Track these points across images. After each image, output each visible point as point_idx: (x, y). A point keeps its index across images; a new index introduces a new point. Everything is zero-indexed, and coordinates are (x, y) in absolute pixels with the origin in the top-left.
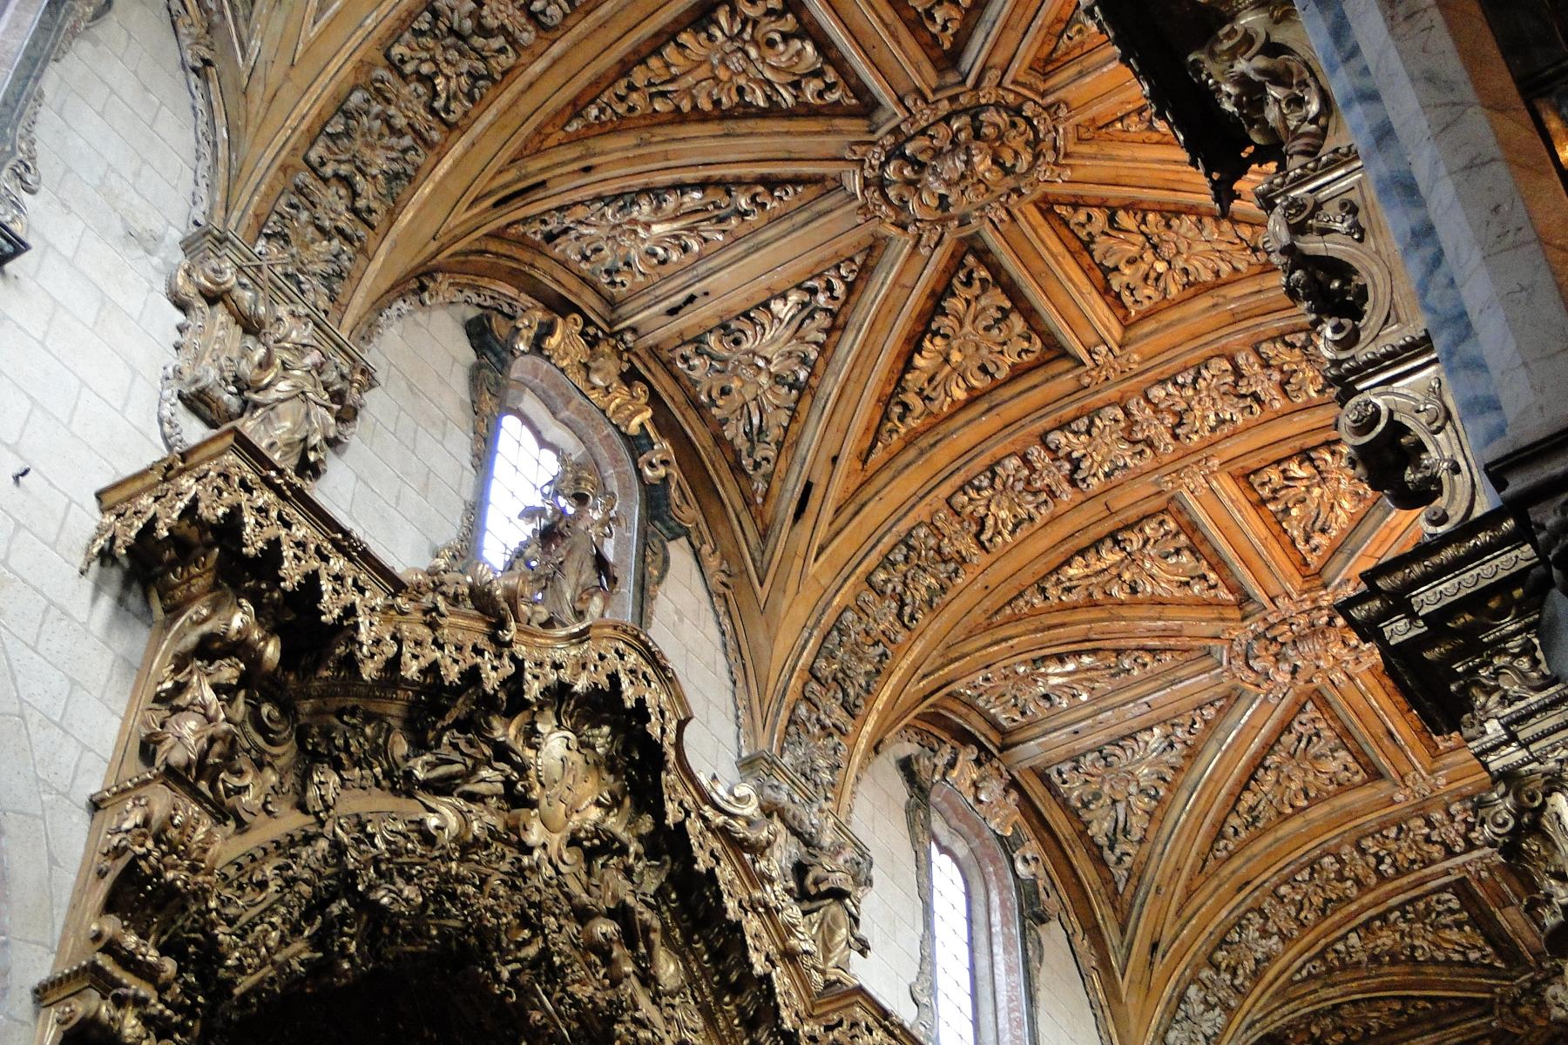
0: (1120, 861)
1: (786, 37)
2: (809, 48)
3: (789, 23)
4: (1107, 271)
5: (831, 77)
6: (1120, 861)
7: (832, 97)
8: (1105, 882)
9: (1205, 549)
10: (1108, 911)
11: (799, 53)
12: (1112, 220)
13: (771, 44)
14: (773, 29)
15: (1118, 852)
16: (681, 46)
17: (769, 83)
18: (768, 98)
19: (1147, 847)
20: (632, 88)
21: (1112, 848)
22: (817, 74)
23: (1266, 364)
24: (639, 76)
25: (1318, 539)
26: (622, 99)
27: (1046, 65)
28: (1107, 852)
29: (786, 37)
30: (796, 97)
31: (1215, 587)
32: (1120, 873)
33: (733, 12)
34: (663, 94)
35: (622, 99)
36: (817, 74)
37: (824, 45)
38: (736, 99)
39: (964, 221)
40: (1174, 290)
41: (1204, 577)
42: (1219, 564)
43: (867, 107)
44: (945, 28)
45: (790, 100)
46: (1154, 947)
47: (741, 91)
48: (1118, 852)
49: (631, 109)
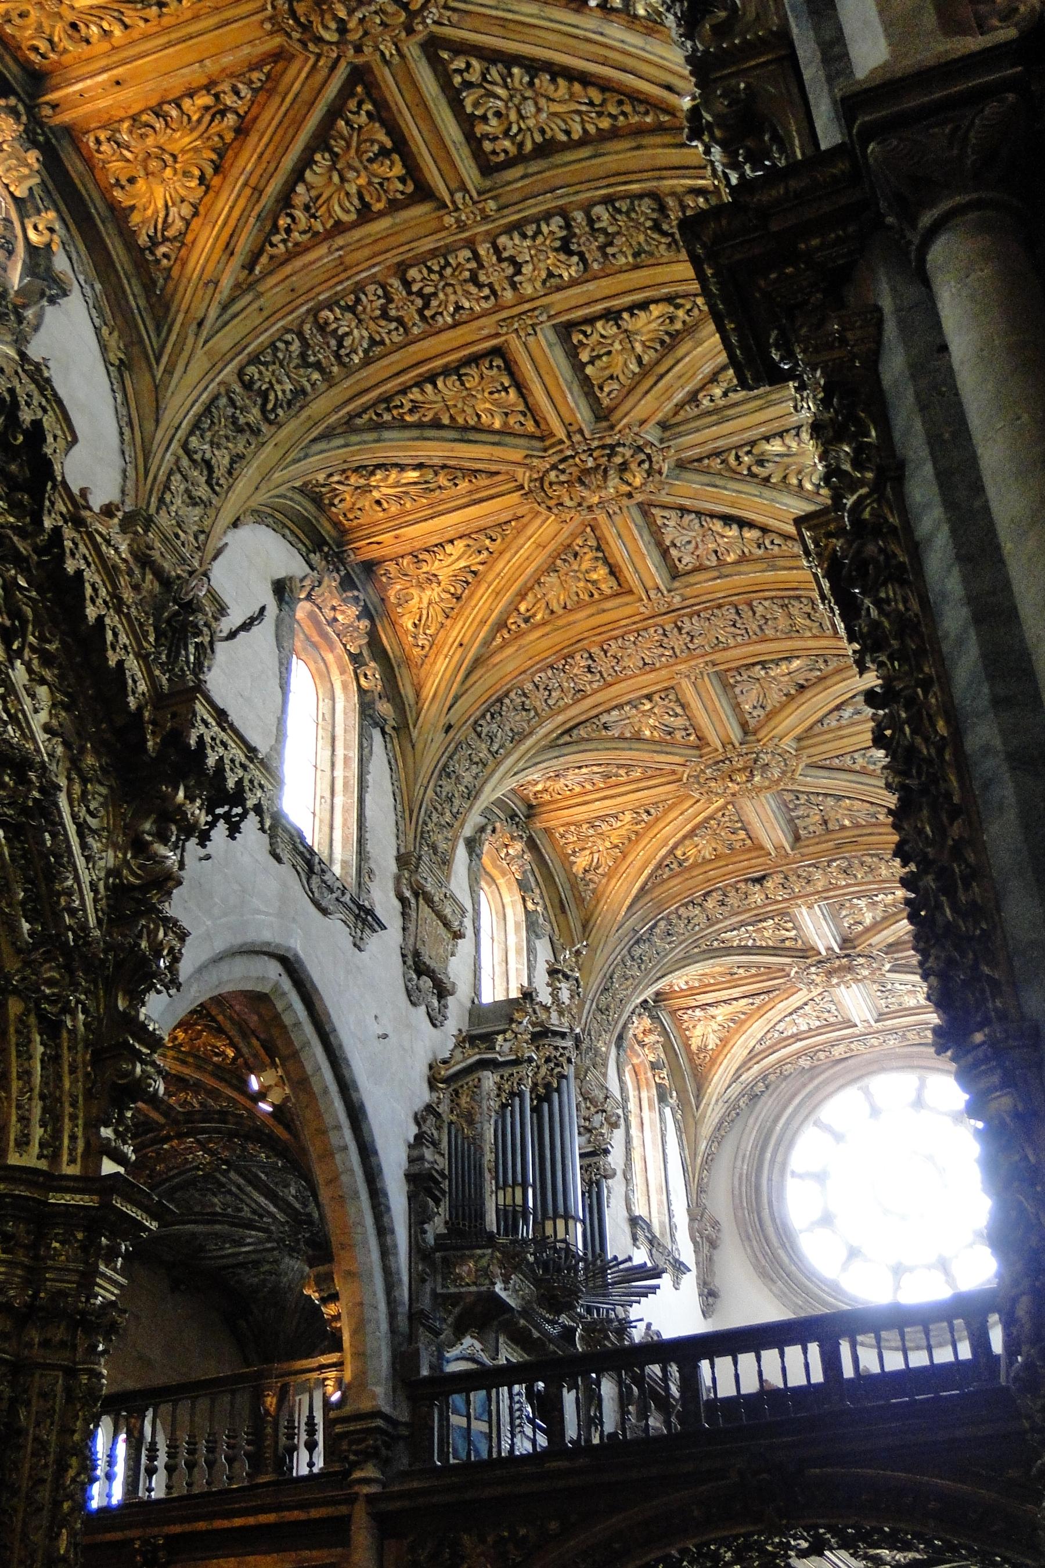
1: (484, 118)
2: (469, 110)
5: (457, 80)
7: (460, 63)
11: (476, 105)
13: (498, 114)
14: (494, 126)
16: (568, 133)
17: (505, 86)
18: (511, 75)
20: (614, 117)
22: (468, 85)
24: (605, 124)
26: (624, 114)
27: (279, 56)
29: (484, 118)
30: (488, 69)
33: (521, 145)
34: (591, 103)
35: (624, 114)
36: (468, 85)
37: (456, 104)
38: (537, 81)
39: (358, 50)
43: (432, 46)
44: (360, 105)
45: (493, 71)
47: (531, 84)
49: (620, 103)
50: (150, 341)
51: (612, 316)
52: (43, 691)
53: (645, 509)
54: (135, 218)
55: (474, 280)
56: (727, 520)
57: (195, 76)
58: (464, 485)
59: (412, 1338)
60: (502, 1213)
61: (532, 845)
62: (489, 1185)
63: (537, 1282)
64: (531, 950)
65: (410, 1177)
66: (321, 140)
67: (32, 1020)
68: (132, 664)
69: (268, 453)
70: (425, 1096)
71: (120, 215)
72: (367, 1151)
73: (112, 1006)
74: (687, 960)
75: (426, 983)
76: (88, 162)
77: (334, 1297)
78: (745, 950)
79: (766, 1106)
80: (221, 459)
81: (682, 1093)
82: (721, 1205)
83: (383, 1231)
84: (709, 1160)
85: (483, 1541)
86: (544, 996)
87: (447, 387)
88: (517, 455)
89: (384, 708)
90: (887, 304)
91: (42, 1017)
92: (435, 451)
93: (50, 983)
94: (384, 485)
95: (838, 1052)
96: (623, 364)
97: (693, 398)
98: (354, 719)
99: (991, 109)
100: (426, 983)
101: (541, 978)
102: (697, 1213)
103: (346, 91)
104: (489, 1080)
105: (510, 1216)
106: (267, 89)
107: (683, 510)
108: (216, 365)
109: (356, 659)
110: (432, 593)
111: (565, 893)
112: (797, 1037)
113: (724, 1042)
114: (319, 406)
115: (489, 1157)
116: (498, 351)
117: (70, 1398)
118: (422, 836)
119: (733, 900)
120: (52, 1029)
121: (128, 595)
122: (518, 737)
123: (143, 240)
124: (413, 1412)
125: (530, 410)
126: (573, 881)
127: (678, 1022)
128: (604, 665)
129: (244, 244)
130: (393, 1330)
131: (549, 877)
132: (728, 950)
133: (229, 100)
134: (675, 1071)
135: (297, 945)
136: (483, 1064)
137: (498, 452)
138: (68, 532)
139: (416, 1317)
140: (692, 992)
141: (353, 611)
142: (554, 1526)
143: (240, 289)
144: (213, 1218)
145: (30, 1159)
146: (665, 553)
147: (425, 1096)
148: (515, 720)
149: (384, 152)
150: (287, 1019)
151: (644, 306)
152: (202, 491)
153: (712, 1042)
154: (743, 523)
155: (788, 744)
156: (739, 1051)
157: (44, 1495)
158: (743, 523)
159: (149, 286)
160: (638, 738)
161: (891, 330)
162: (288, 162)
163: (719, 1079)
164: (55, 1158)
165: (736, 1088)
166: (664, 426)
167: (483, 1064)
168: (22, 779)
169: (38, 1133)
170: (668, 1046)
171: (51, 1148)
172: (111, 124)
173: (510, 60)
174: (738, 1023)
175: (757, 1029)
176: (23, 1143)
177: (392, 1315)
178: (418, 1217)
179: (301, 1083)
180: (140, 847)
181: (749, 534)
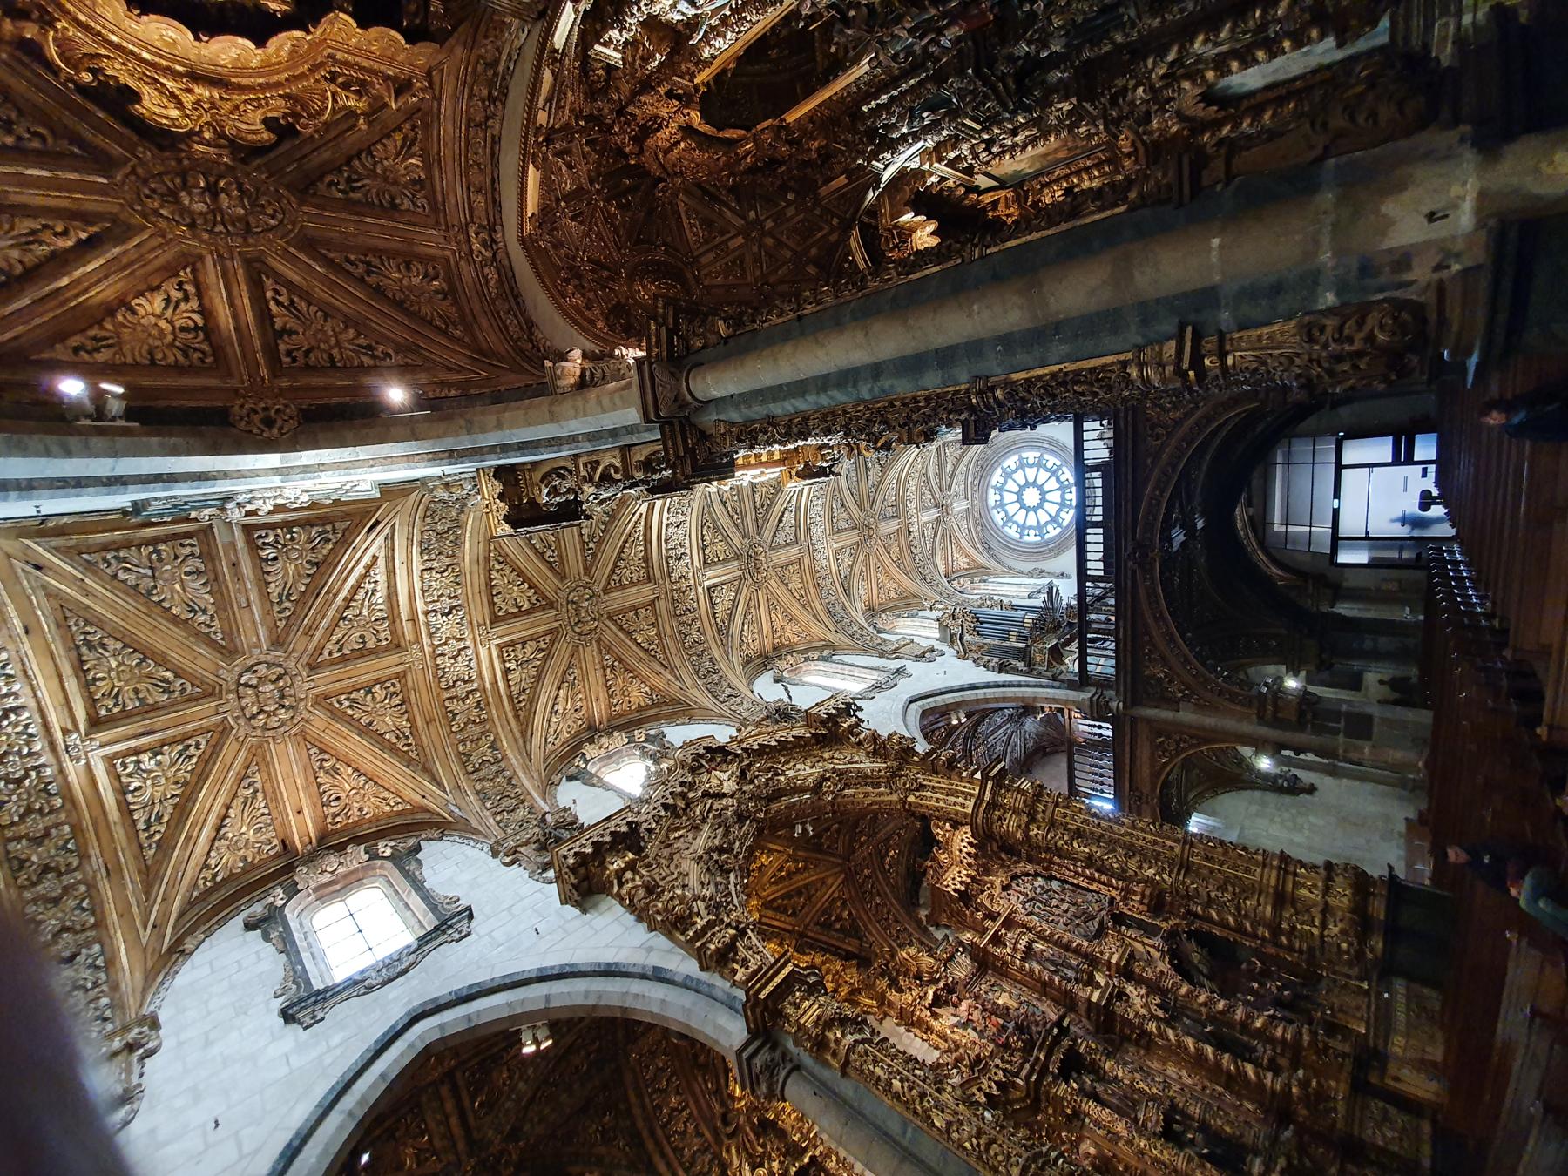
0: (105, 560)
3: (635, 580)
4: (524, 644)
6: (105, 560)
8: (89, 547)
9: (357, 654)
10: (72, 543)
12: (543, 650)
14: (635, 576)
15: (113, 561)
19: (107, 578)
21: (114, 557)
23: (469, 692)
25: (347, 703)
27: (599, 641)
28: (113, 554)
31: (330, 654)
32: (96, 557)
40: (508, 665)
41: (339, 651)
42: (344, 659)
46: (38, 568)
48: (113, 561)
50: (684, 707)
51: (704, 548)
52: (798, 766)
53: (771, 548)
54: (642, 704)
55: (684, 592)
56: (780, 521)
57: (599, 674)
58: (752, 610)
59: (1062, 681)
60: (1018, 640)
61: (884, 611)
62: (1008, 644)
63: (1048, 632)
64: (922, 618)
65: (1000, 672)
66: (629, 634)
67: (917, 794)
68: (795, 732)
69: (730, 675)
70: (970, 662)
71: (640, 709)
72: (987, 686)
73: (916, 764)
74: (934, 564)
75: (927, 655)
76: (621, 716)
77: (1042, 708)
78: (934, 542)
79: (994, 545)
80: (729, 691)
81: (983, 574)
82: (1028, 567)
83: (1019, 685)
84: (1010, 568)
85: (1148, 667)
86: (940, 613)
87: (719, 608)
88: (745, 589)
89: (825, 653)
90: (714, 417)
91: (918, 790)
92: (739, 617)
93: (905, 784)
94: (748, 638)
95: (977, 516)
96: (720, 547)
97: (737, 525)
98: (827, 664)
99: (657, 373)
100: (927, 655)
101: (934, 614)
102: (1030, 575)
103: (615, 623)
104: (967, 637)
105: (1020, 638)
106: (609, 650)
107: (774, 535)
108: (697, 687)
109: (807, 660)
110: (788, 627)
111: (903, 602)
112: (969, 529)
113: (967, 556)
114: (716, 654)
115: (996, 642)
116: (709, 589)
117: (1067, 807)
118: (874, 648)
119: (915, 543)
120: (922, 787)
121: (770, 729)
122: (844, 608)
123: (650, 703)
124: (1091, 685)
125: (730, 582)
126: (899, 599)
127: (957, 571)
128: (823, 573)
129: (658, 668)
130: (1059, 688)
131: (897, 607)
132: (933, 549)
133: (610, 662)
134: (975, 575)
135: (906, 696)
136: (961, 639)
137: (743, 595)
138: (744, 746)
139: (1054, 678)
140: (946, 564)
141: (789, 657)
142: (1146, 638)
143: (672, 673)
144: (1005, 751)
145: (970, 804)
146: (787, 545)
147: (970, 662)
148: (838, 608)
149: (636, 614)
150: (933, 705)
151: (703, 536)
152: (738, 699)
153: (966, 560)
154: (782, 516)
155: (862, 514)
156: (972, 551)
157: (1104, 824)
158: (782, 516)
159: (665, 704)
160: (851, 566)
161: (722, 417)
162: (634, 647)
163: (981, 560)
164: (972, 795)
165: (985, 554)
166: (744, 537)
167: (961, 639)
168: (828, 779)
169: (960, 800)
170: (965, 576)
171: (967, 796)
172: (610, 705)
173: (615, 566)
174: (961, 549)
175: (964, 542)
176: (963, 806)
177: (1053, 687)
178: (1016, 671)
179: (957, 706)
180: (860, 743)
181: (787, 514)
